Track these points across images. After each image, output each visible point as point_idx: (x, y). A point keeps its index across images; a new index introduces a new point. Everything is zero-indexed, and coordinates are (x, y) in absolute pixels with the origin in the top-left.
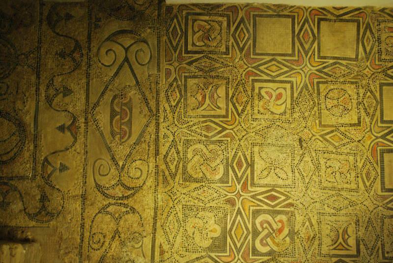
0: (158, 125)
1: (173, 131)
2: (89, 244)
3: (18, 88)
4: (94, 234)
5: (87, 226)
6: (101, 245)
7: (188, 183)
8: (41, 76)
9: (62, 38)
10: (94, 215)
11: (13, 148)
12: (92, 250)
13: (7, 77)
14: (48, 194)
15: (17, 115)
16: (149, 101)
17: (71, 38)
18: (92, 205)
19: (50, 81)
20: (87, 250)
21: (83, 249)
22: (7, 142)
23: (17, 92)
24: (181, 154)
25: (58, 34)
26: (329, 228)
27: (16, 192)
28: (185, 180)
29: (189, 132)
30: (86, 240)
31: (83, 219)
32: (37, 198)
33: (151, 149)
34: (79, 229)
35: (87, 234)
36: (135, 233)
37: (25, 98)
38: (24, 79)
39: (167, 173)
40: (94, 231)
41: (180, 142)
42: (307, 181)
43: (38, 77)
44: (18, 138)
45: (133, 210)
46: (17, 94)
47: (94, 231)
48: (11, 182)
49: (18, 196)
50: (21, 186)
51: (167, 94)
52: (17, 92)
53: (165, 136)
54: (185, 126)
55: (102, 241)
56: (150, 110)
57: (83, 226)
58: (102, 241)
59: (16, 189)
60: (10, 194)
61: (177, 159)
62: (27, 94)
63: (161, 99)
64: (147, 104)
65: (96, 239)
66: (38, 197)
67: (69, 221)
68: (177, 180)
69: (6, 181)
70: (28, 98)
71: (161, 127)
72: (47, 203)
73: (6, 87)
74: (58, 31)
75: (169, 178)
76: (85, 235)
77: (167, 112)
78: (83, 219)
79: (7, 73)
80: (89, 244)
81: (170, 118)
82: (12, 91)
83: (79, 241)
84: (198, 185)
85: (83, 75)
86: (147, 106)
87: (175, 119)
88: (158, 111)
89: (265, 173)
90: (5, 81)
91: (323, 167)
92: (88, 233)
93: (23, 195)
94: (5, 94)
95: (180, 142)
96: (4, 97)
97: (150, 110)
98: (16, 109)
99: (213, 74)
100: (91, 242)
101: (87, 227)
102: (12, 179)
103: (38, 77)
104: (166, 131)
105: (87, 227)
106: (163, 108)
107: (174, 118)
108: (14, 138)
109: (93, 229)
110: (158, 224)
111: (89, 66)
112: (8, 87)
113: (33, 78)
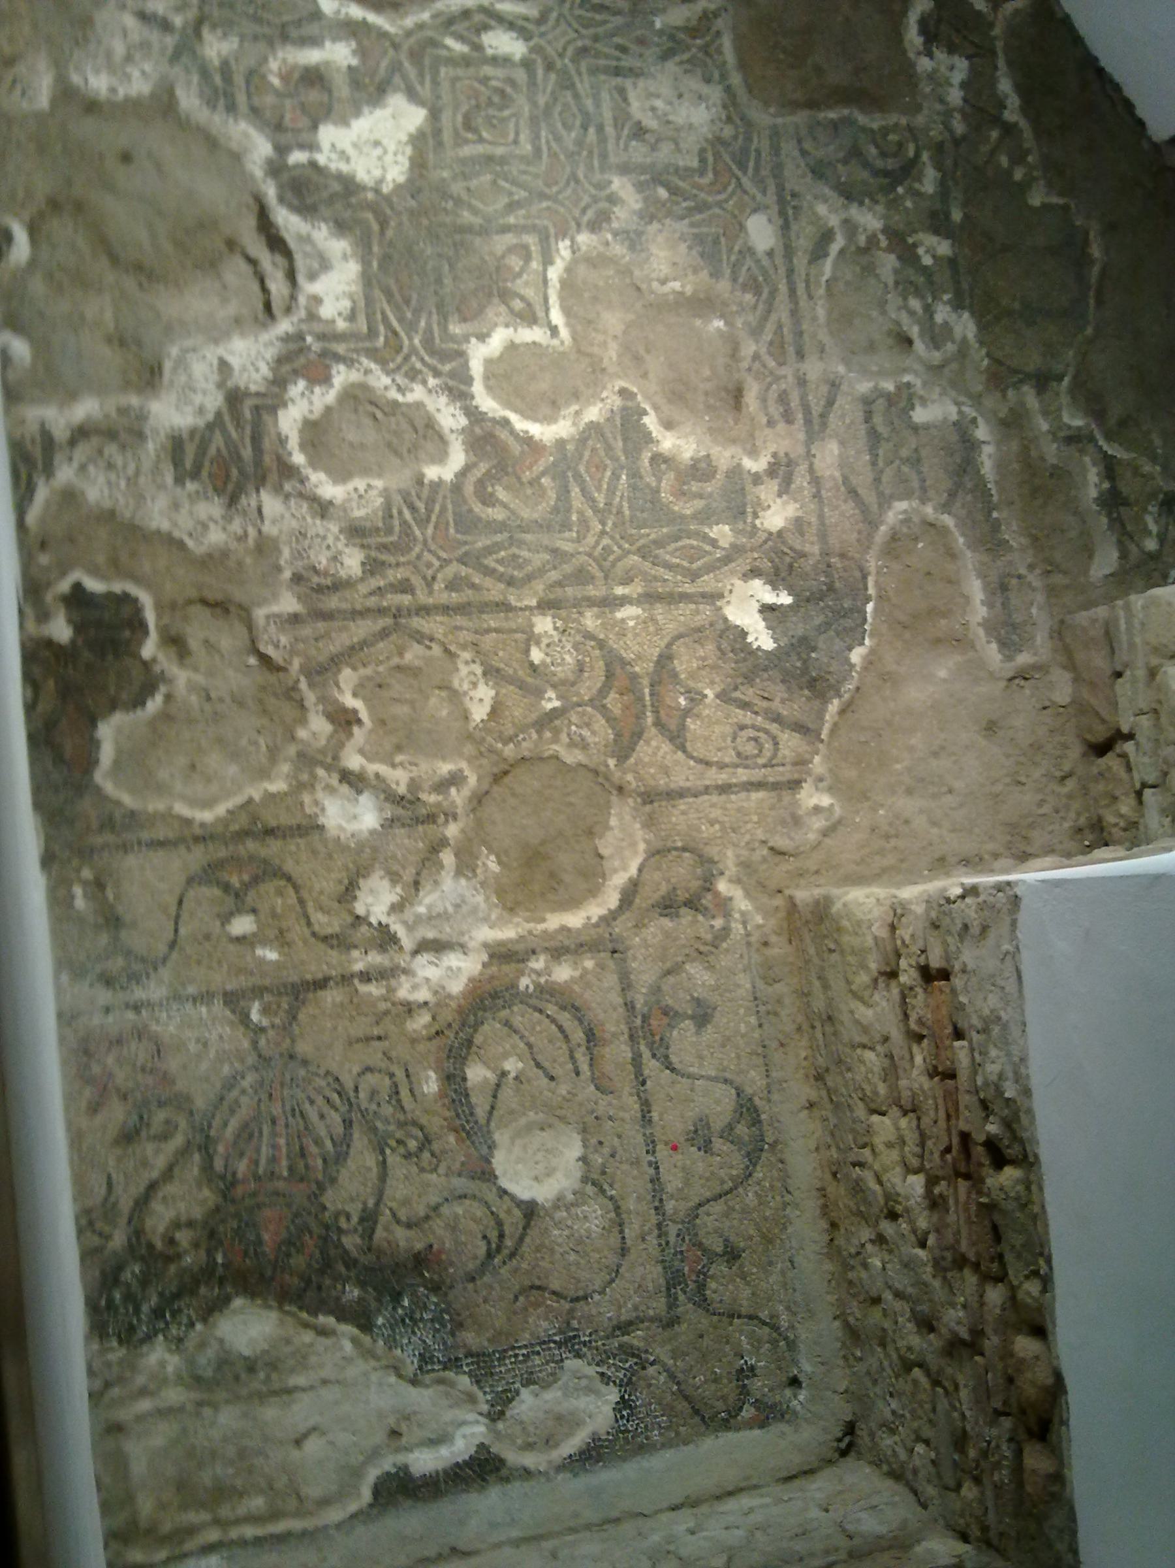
0: (424, 610)
1: (437, 563)
2: (765, 766)
3: (368, 1039)
4: (739, 754)
5: (722, 777)
6: (761, 734)
7: (574, 518)
8: (320, 976)
9: (182, 931)
10: (692, 763)
11: (548, 1016)
12: (780, 755)
13: (337, 1079)
14: (656, 897)
15: (450, 1025)
16: (355, 640)
17: (180, 902)
18: (667, 774)
19: (332, 947)
20: (781, 769)
21: (780, 778)
22: (532, 1039)
23: (379, 1038)
24: (499, 538)
25: (173, 945)
26: (634, 143)
27: (665, 988)
28: (566, 526)
29: (434, 518)
30: (757, 775)
31: (707, 790)
32: (671, 924)
33: (493, 624)
34: (733, 797)
35: (743, 775)
36: (719, 649)
37: (394, 1011)
38: (335, 1028)
39: (554, 575)
40: (729, 757)
41: (466, 543)
42: (523, 194)
43: (321, 984)
44: (515, 1009)
45: (665, 659)
46: (386, 1038)
47: (729, 757)
48: (638, 1006)
49: (671, 979)
50: (645, 977)
51: (328, 588)
52: (379, 1038)
53: (451, 586)
54: (417, 533)
55: (752, 733)
56: (384, 634)
57: (724, 789)
58: (752, 733)
59: (656, 990)
60: (670, 1002)
61: (515, 550)
62: (383, 1006)
63: (344, 606)
64: (364, 644)
65: (750, 749)
66: (667, 923)
67: (717, 827)
68: (568, 547)
69: (638, 1021)
70: (393, 1004)
71: (423, 598)
72: (682, 895)
73: (369, 1076)
74: (162, 948)
75: (568, 568)
76: (745, 778)
77: (382, 583)
78: (707, 790)
79: (323, 1083)
80: (765, 766)
81: (400, 574)
82: (380, 1055)
83: (761, 795)
84: (575, 491)
85: (298, 848)
86: (372, 645)
87: (402, 559)
88: (381, 611)
89: (518, 305)
90: (349, 1085)
91: (480, 149)
92: (740, 770)
93: (668, 965)
94: (392, 1075)
95: (466, 543)
96: (400, 1074)
97: (384, 634)
98: (433, 1031)
99: (247, 453)
100: (761, 761)
101: (724, 776)
102: (630, 1006)
103: (321, 984)
104: (438, 586)
105: (724, 776)
106: (373, 598)
107: (398, 565)
108: (517, 1021)
109: (727, 760)
110: (688, 588)
111: (270, 832)
112: (368, 1069)
113: (332, 997)
